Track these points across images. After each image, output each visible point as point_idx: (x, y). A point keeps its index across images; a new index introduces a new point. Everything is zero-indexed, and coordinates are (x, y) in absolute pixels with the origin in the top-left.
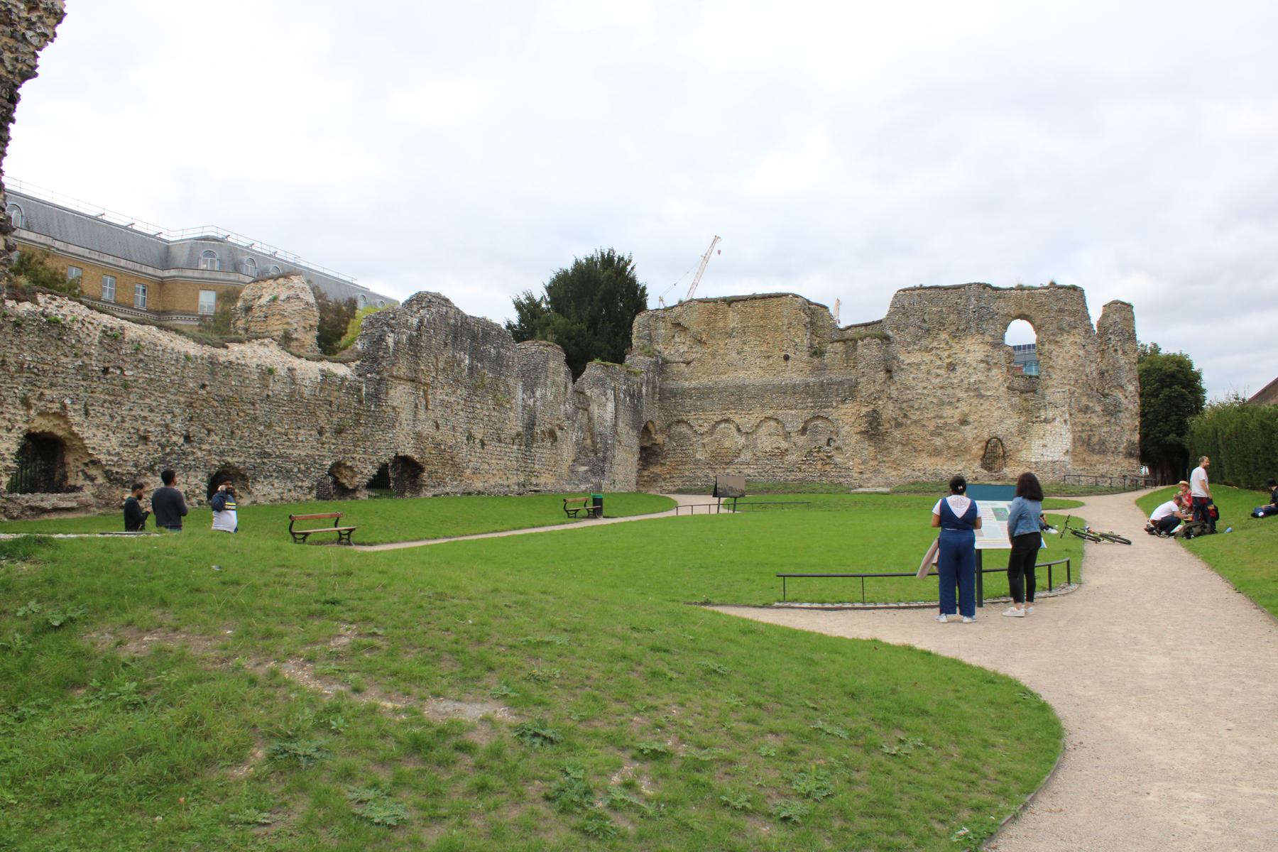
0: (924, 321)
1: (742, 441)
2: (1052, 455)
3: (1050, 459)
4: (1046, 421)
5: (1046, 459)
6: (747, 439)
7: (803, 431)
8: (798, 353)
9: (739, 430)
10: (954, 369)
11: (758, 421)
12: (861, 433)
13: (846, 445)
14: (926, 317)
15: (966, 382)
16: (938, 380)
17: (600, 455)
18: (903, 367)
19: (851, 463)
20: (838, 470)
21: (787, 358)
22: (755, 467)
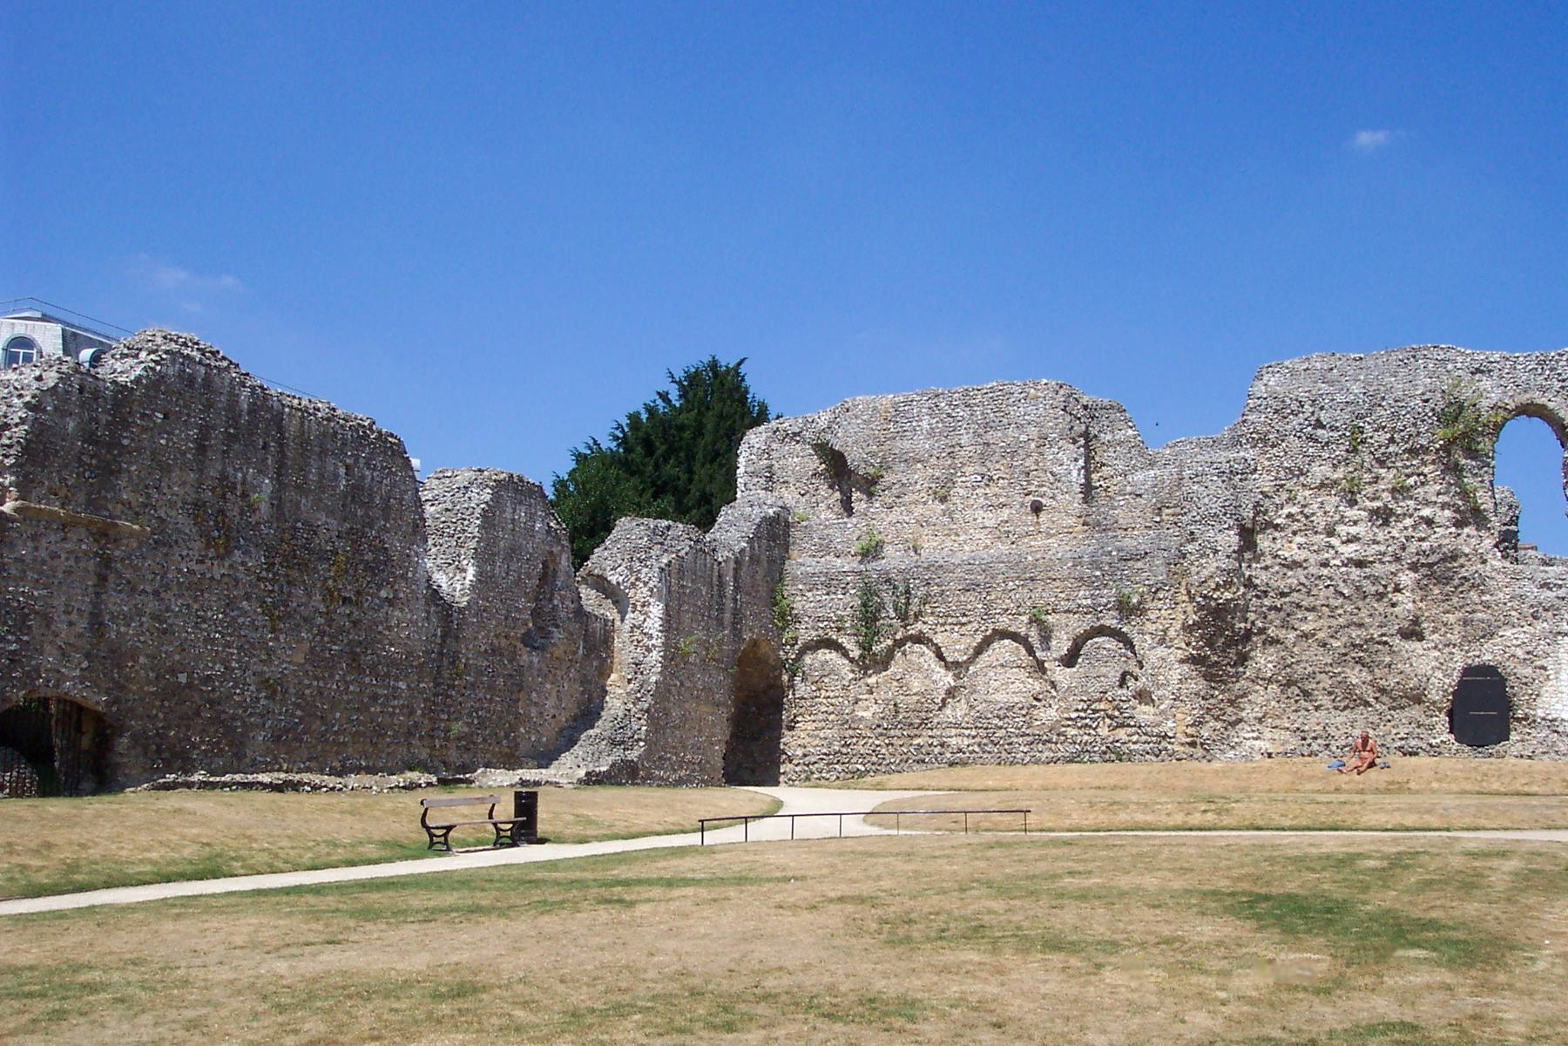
0: (1319, 425)
1: (948, 679)
6: (957, 677)
7: (1070, 660)
8: (1059, 497)
10: (1386, 523)
11: (979, 638)
12: (1192, 660)
13: (1159, 686)
14: (1324, 416)
15: (1413, 547)
16: (1353, 547)
18: (1278, 521)
19: (1170, 724)
20: (1144, 738)
21: (1037, 508)
22: (974, 733)
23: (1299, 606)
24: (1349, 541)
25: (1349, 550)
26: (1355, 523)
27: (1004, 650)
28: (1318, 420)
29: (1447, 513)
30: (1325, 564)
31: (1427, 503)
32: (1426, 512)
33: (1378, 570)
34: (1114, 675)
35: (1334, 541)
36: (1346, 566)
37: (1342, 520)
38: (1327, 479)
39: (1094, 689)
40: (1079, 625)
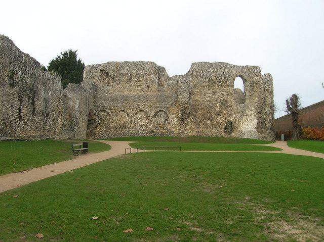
7: (154, 116)
9: (128, 114)
10: (215, 94)
15: (219, 99)
17: (73, 123)
21: (148, 87)
27: (141, 114)
30: (204, 101)
31: (223, 91)
32: (222, 93)
33: (213, 103)
34: (163, 120)
39: (159, 122)
40: (156, 110)
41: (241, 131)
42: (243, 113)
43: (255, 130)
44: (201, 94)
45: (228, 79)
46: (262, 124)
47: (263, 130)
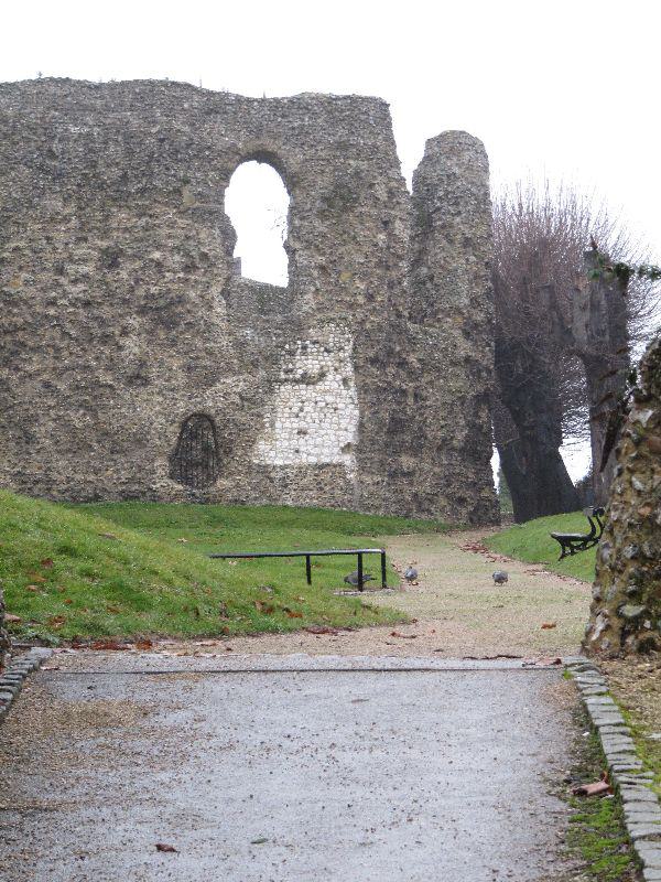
2: (317, 450)
3: (313, 460)
4: (306, 379)
5: (305, 459)
10: (114, 265)
14: (56, 146)
16: (81, 287)
23: (23, 345)
24: (75, 282)
25: (77, 290)
26: (85, 261)
28: (50, 151)
29: (177, 258)
30: (52, 303)
32: (157, 255)
35: (63, 280)
36: (74, 305)
37: (71, 260)
38: (58, 213)
41: (265, 470)
42: (269, 369)
43: (348, 460)
44: (37, 265)
45: (186, 182)
46: (397, 425)
47: (407, 462)
